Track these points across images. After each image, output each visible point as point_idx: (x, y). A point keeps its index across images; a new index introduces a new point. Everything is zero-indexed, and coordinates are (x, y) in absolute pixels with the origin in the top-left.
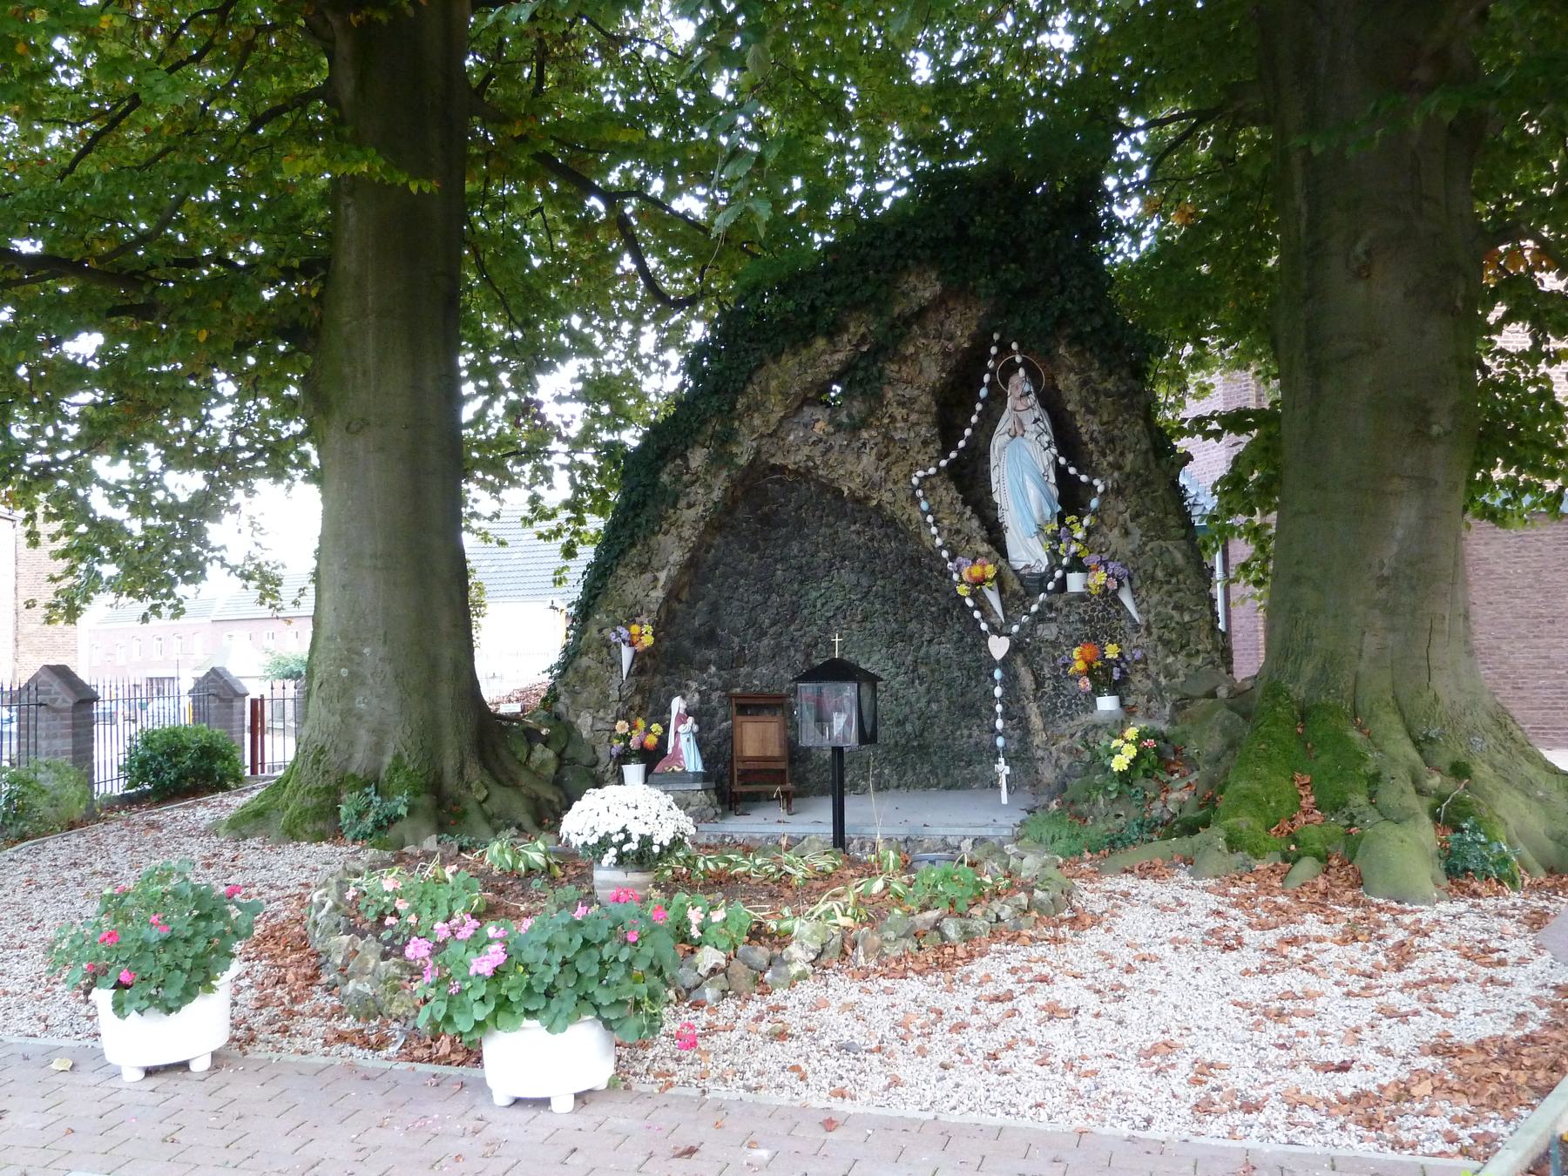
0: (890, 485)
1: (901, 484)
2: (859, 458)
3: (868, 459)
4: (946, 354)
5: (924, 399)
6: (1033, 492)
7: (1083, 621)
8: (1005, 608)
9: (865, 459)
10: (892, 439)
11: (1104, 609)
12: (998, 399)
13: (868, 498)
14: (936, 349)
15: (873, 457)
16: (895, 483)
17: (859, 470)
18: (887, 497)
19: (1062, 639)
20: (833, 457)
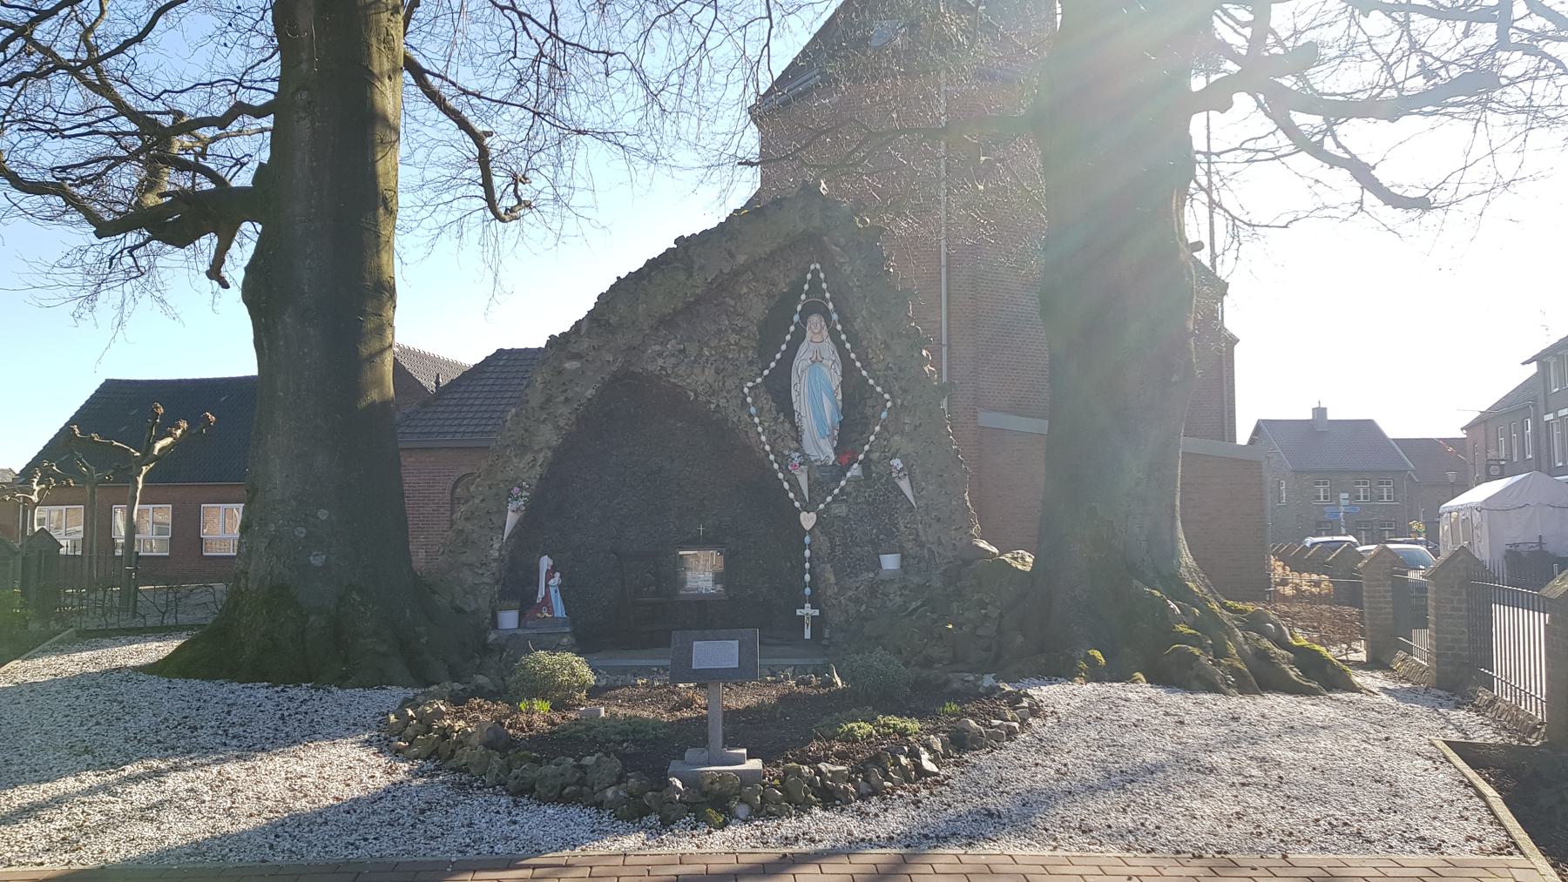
1: (734, 393)
3: (709, 373)
4: (770, 296)
6: (827, 404)
12: (800, 337)
18: (723, 402)
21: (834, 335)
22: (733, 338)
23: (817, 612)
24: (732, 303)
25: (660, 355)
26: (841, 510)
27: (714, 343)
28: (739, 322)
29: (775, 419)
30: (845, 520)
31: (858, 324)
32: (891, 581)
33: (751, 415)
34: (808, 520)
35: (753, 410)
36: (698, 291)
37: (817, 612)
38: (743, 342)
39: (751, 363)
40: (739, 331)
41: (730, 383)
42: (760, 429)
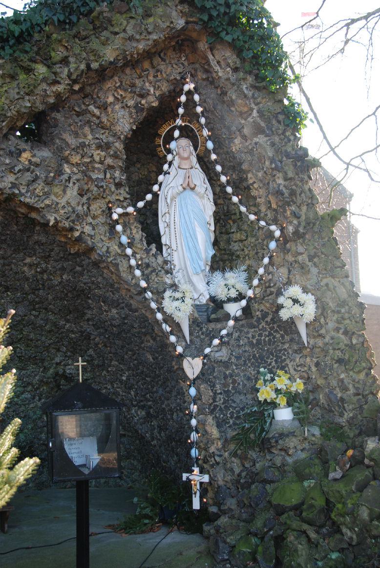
0: (90, 220)
2: (64, 191)
3: (72, 192)
4: (138, 108)
5: (119, 146)
7: (251, 344)
8: (191, 334)
9: (69, 192)
10: (90, 178)
11: (270, 334)
13: (72, 229)
14: (131, 103)
15: (75, 193)
16: (94, 217)
17: (63, 202)
18: (88, 229)
19: (233, 360)
20: (39, 188)
21: (204, 162)
22: (98, 155)
23: (206, 478)
24: (97, 112)
25: (11, 170)
26: (223, 354)
27: (76, 159)
28: (105, 137)
29: (148, 251)
30: (226, 364)
31: (237, 144)
32: (292, 434)
33: (121, 245)
34: (193, 367)
35: (124, 240)
36: (60, 88)
37: (206, 478)
38: (109, 161)
39: (118, 185)
40: (104, 146)
41: (97, 207)
42: (133, 262)
